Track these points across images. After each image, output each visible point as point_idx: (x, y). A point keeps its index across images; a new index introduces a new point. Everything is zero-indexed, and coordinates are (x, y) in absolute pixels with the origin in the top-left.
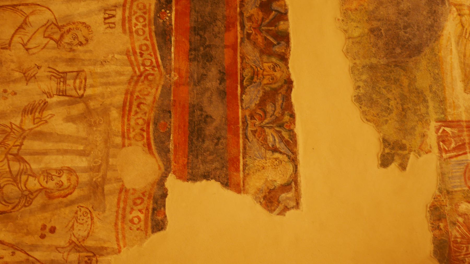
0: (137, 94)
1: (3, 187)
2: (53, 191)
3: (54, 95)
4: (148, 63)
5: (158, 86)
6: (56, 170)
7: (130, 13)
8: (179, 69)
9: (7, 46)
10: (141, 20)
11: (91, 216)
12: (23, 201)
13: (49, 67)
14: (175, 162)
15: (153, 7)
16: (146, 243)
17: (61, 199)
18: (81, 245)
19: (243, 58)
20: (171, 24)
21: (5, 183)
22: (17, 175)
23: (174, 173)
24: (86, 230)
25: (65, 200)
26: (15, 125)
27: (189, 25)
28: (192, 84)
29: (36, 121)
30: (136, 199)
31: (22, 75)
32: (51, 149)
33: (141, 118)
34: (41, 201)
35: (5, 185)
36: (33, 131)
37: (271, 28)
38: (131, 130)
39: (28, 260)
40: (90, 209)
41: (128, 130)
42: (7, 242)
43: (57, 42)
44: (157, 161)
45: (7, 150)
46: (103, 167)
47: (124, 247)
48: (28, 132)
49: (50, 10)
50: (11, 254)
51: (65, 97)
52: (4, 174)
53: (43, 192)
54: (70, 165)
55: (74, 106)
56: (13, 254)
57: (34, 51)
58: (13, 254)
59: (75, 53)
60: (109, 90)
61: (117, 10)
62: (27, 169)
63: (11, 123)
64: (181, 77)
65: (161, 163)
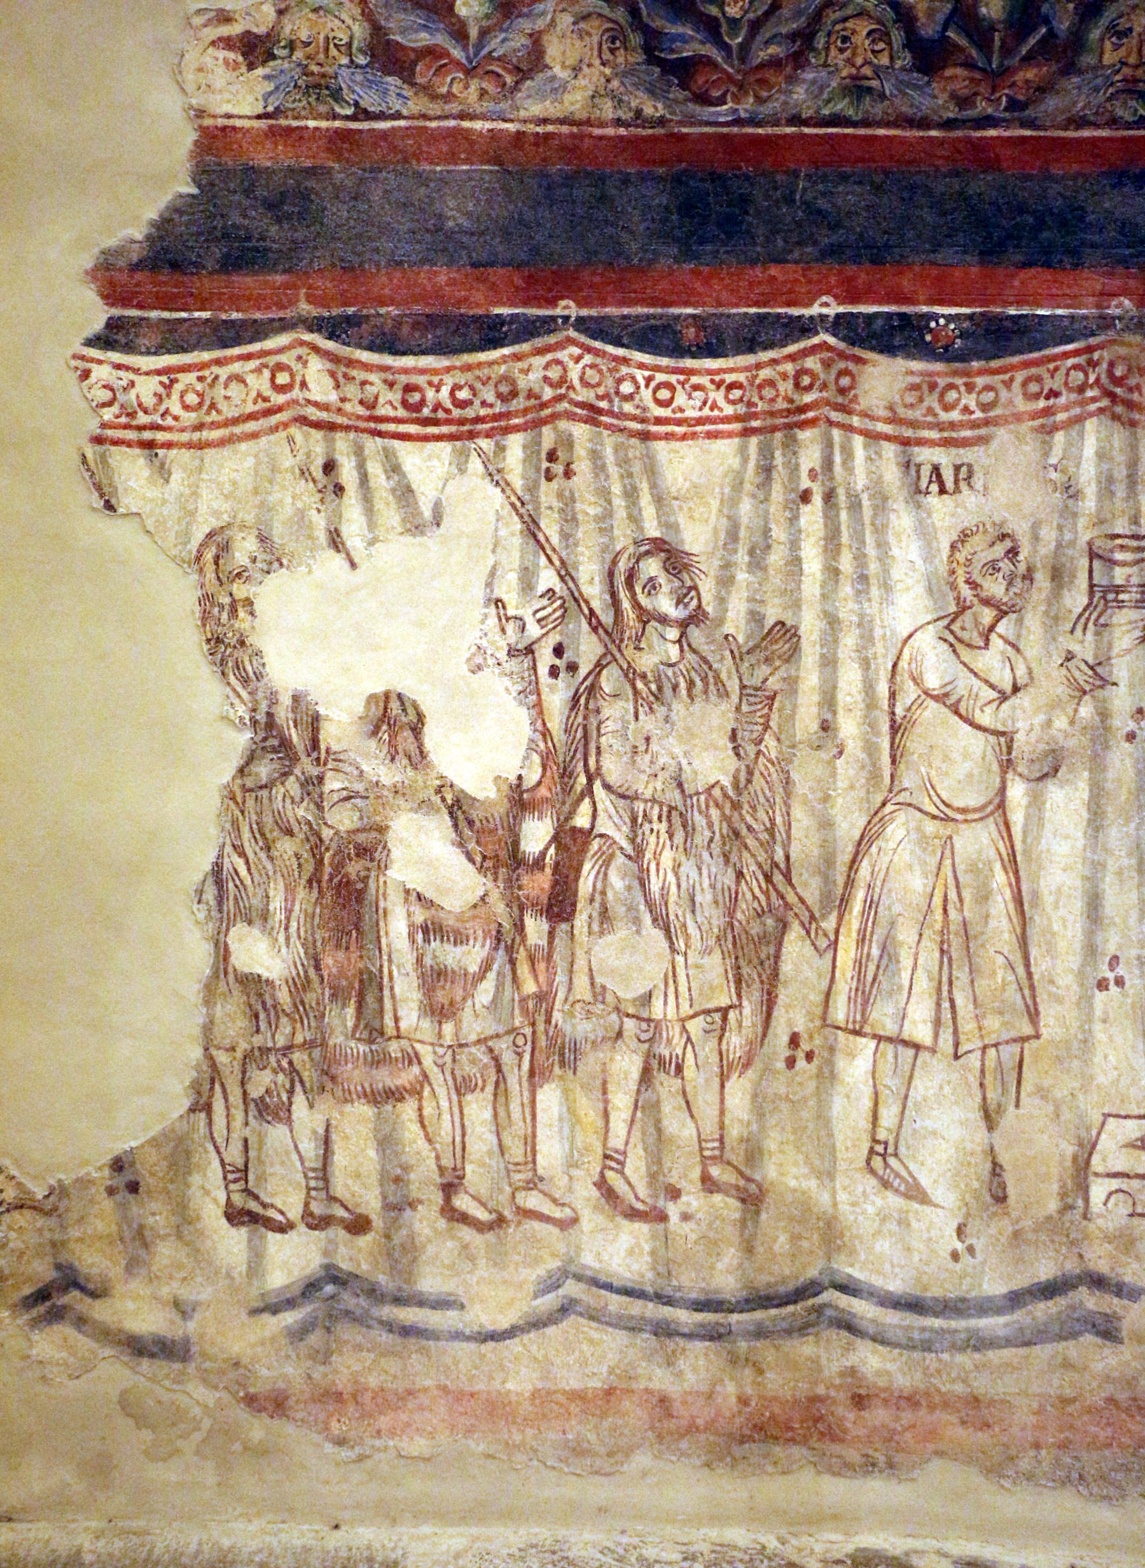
4: (1078, 377)
7: (930, 426)
8: (1102, 294)
9: (1002, 740)
10: (952, 395)
13: (1072, 632)
15: (916, 365)
19: (1081, 122)
20: (971, 317)
27: (975, 270)
31: (1087, 698)
37: (997, 43)
43: (1002, 614)
49: (910, 636)
57: (1021, 671)
59: (1039, 565)
61: (918, 460)
64: (1124, 292)
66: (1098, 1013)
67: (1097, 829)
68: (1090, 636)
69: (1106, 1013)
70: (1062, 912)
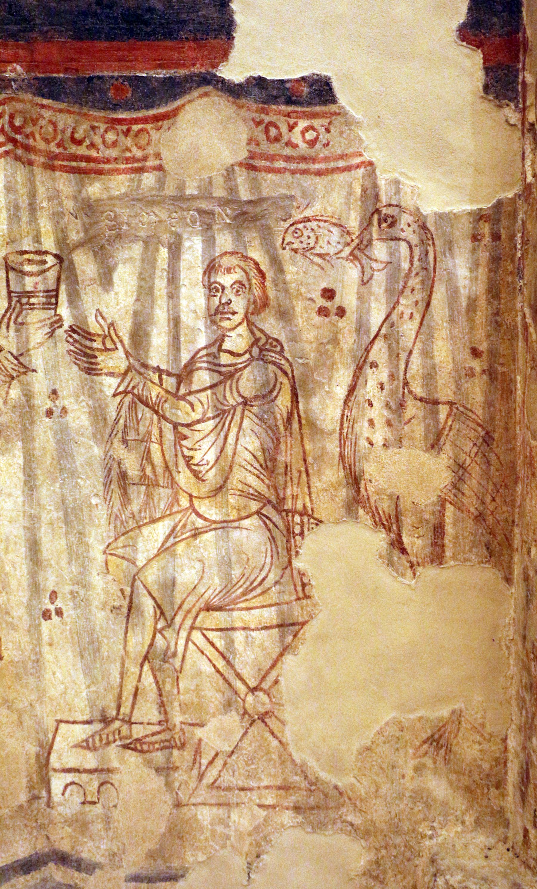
0: (53, 148)
1: (243, 397)
2: (252, 300)
3: (56, 315)
5: (37, 104)
6: (209, 297)
11: (301, 222)
12: (272, 356)
14: (194, 65)
16: (354, 114)
17: (268, 284)
18: (357, 237)
21: (236, 394)
22: (219, 372)
23: (215, 66)
24: (329, 231)
25: (269, 275)
26: (119, 386)
28: (30, 34)
29: (109, 345)
30: (268, 138)
31: (15, 382)
32: (168, 310)
33: (103, 137)
34: (272, 321)
35: (240, 395)
36: (130, 351)
38: (128, 154)
39: (385, 337)
40: (287, 225)
41: (127, 160)
42: (351, 378)
44: (190, 101)
45: (169, 397)
46: (204, 205)
47: (361, 155)
48: (131, 360)
50: (374, 369)
51: (60, 292)
52: (217, 399)
53: (253, 318)
54: (201, 271)
55: (79, 272)
56: (374, 365)
58: (374, 365)
60: (44, 204)
62: (207, 355)
63: (114, 395)
64: (16, 59)
65: (195, 94)
66: (45, 638)
67: (31, 489)
68: (12, 333)
69: (51, 638)
70: (11, 556)
